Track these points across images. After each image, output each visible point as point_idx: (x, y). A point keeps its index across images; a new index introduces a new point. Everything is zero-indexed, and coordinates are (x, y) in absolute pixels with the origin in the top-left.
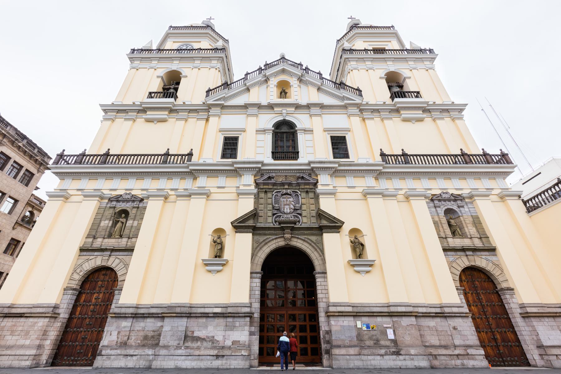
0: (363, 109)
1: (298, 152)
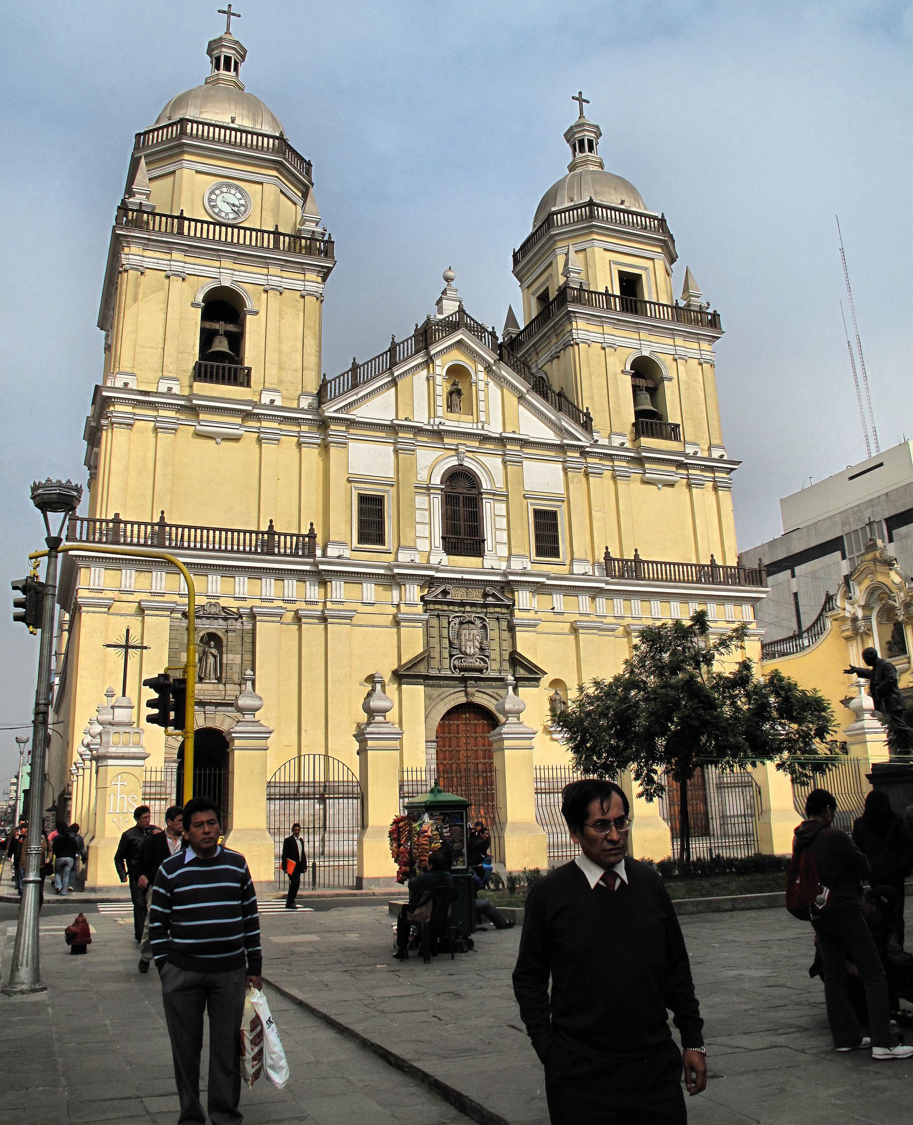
0: (589, 452)
1: (484, 541)
